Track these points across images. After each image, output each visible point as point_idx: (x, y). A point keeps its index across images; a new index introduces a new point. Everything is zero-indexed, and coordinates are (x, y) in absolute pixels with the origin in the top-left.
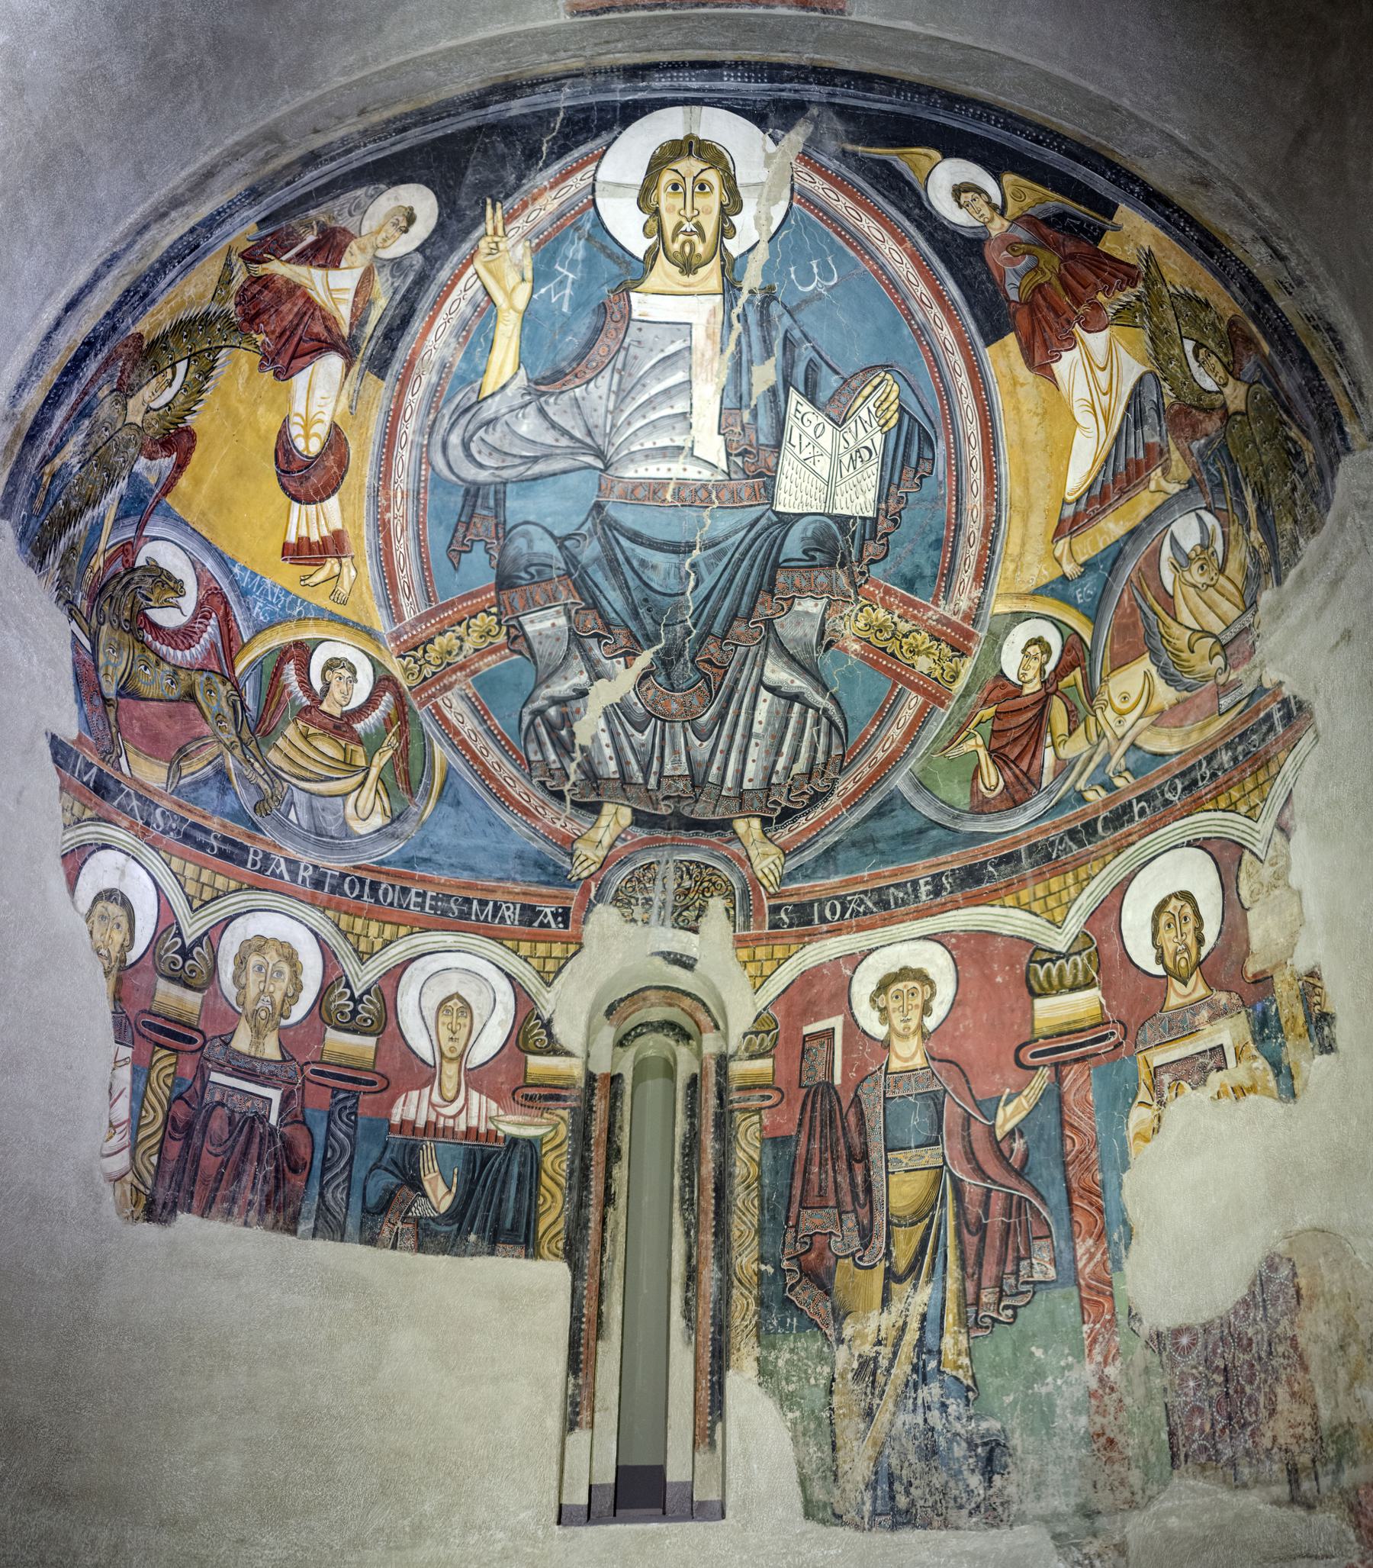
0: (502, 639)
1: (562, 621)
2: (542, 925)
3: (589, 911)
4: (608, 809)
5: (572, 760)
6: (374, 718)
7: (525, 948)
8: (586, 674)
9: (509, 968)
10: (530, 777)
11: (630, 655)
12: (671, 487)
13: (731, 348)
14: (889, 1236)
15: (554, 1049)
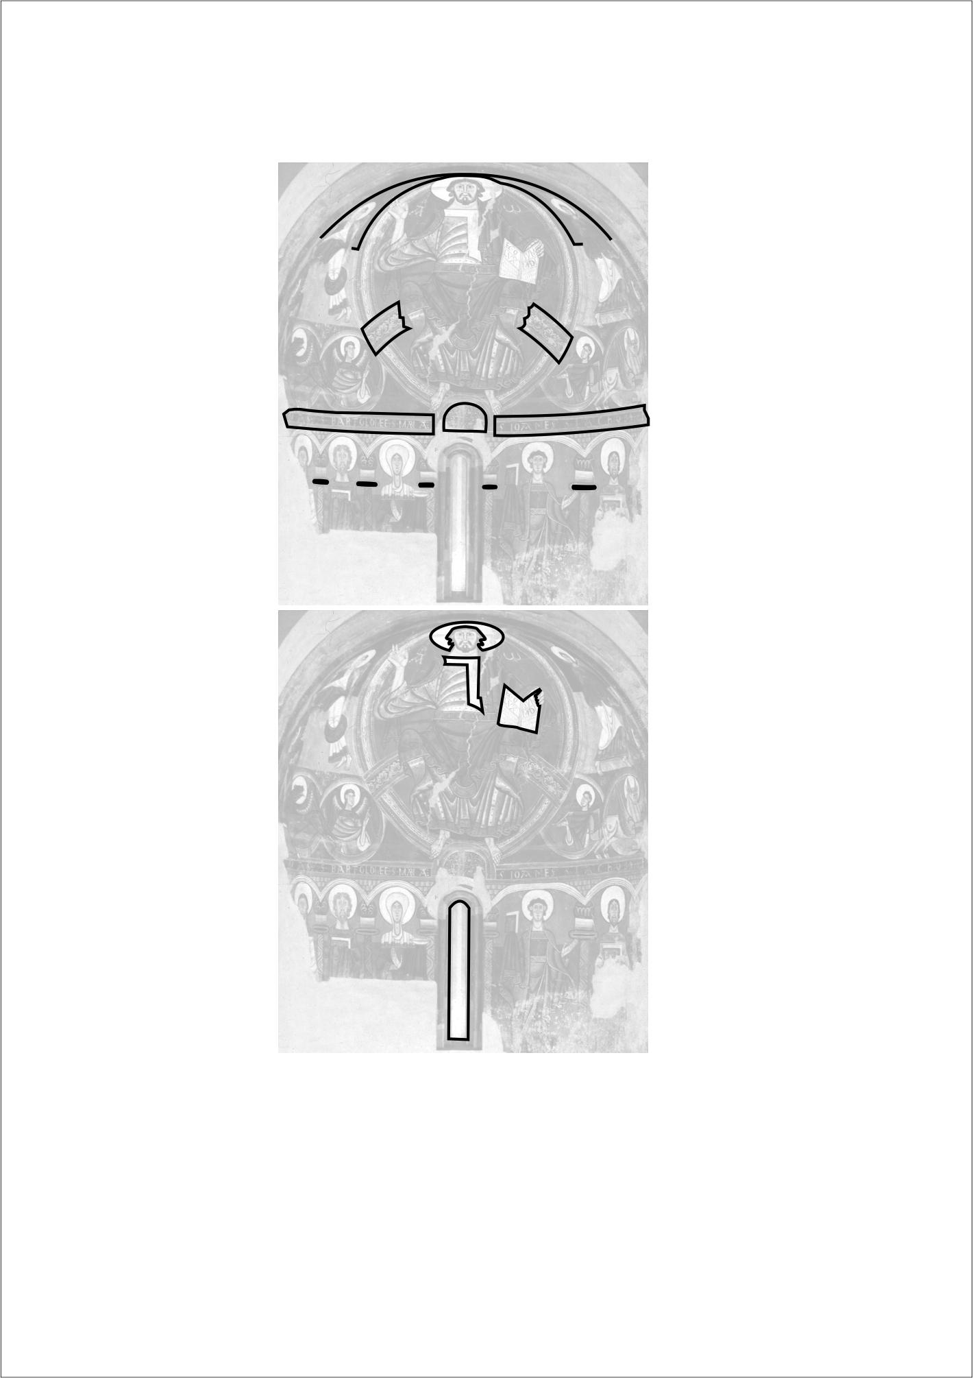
0: (402, 770)
1: (423, 762)
2: (422, 875)
3: (437, 870)
4: (442, 832)
5: (429, 813)
6: (362, 807)
7: (417, 884)
8: (431, 782)
9: (413, 891)
10: (414, 821)
11: (447, 774)
12: (461, 714)
13: (482, 224)
14: (530, 980)
15: (428, 917)
